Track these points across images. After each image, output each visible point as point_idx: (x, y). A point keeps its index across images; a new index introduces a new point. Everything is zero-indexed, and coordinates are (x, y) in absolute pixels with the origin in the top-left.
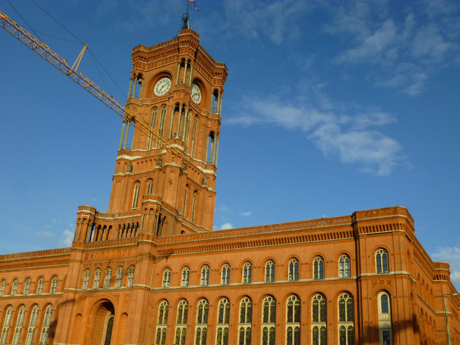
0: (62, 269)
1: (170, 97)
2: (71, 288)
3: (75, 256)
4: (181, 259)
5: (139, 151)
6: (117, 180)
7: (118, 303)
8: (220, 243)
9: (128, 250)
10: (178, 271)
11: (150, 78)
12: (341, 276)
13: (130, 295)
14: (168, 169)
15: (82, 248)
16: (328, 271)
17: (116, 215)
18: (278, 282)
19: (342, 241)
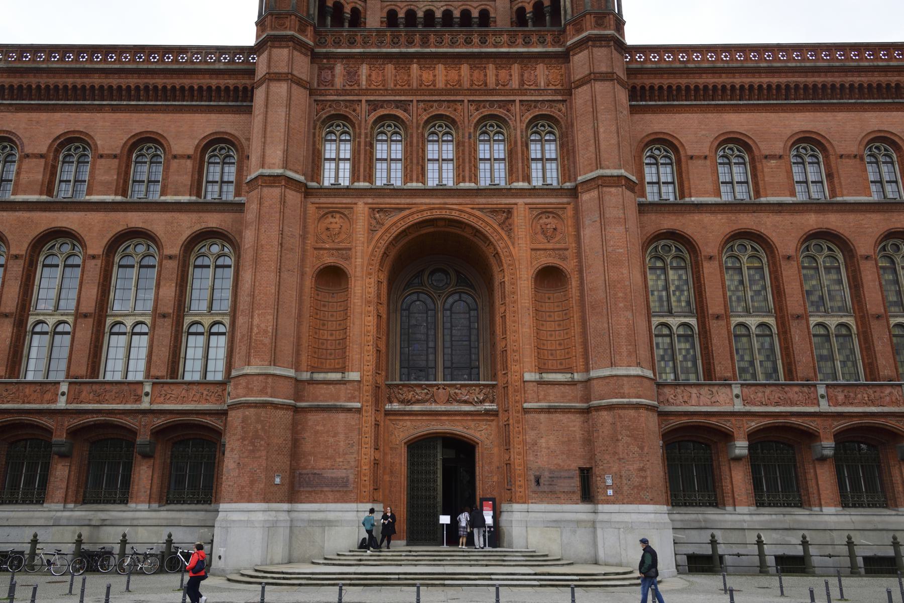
0: (187, 117)
2: (290, 170)
3: (291, 61)
7: (510, 237)
9: (516, 68)
13: (560, 213)
15: (310, 39)
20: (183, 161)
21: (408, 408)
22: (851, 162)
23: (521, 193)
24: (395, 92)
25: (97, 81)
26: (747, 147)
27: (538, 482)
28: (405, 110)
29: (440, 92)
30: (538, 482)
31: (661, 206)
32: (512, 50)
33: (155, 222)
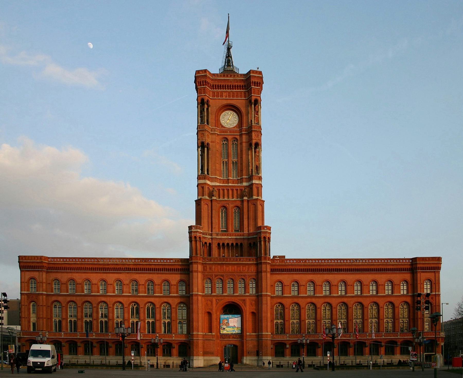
0: (174, 275)
1: (244, 133)
4: (291, 276)
5: (217, 178)
6: (205, 203)
7: (245, 306)
8: (323, 267)
10: (289, 284)
11: (217, 108)
12: (402, 293)
14: (258, 202)
16: (395, 290)
17: (213, 234)
18: (365, 295)
19: (403, 273)
20: (174, 286)
21: (224, 339)
22: (319, 287)
23: (247, 296)
24: (220, 272)
25: (153, 267)
26: (298, 283)
27: (248, 353)
28: (223, 277)
29: (230, 273)
30: (248, 353)
31: (278, 297)
32: (246, 263)
33: (170, 300)
